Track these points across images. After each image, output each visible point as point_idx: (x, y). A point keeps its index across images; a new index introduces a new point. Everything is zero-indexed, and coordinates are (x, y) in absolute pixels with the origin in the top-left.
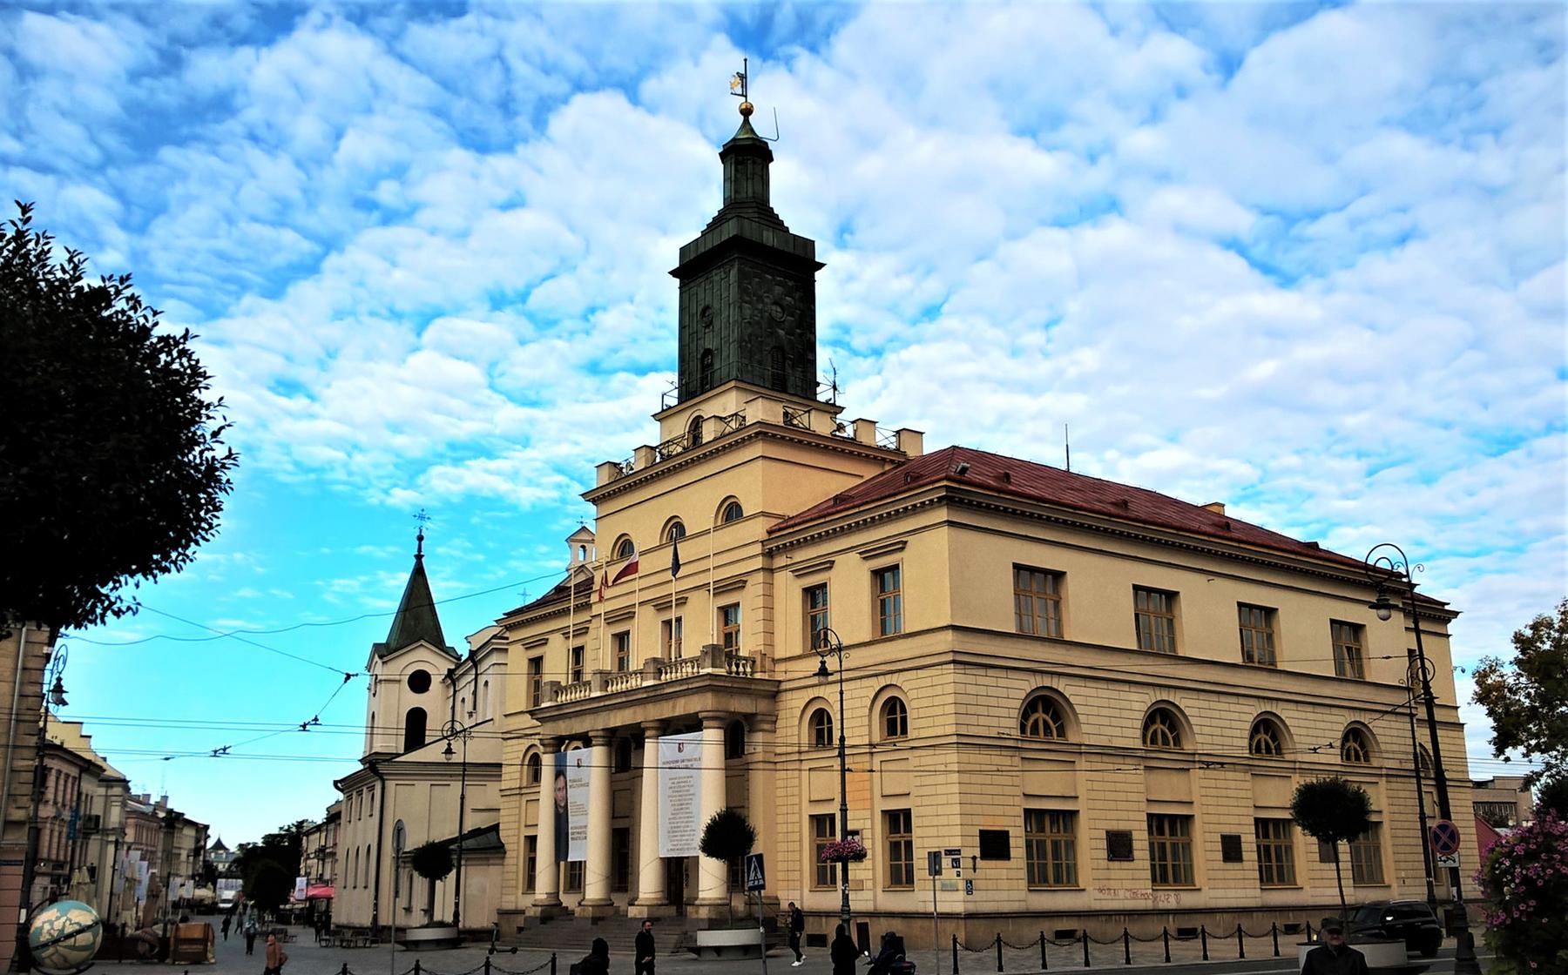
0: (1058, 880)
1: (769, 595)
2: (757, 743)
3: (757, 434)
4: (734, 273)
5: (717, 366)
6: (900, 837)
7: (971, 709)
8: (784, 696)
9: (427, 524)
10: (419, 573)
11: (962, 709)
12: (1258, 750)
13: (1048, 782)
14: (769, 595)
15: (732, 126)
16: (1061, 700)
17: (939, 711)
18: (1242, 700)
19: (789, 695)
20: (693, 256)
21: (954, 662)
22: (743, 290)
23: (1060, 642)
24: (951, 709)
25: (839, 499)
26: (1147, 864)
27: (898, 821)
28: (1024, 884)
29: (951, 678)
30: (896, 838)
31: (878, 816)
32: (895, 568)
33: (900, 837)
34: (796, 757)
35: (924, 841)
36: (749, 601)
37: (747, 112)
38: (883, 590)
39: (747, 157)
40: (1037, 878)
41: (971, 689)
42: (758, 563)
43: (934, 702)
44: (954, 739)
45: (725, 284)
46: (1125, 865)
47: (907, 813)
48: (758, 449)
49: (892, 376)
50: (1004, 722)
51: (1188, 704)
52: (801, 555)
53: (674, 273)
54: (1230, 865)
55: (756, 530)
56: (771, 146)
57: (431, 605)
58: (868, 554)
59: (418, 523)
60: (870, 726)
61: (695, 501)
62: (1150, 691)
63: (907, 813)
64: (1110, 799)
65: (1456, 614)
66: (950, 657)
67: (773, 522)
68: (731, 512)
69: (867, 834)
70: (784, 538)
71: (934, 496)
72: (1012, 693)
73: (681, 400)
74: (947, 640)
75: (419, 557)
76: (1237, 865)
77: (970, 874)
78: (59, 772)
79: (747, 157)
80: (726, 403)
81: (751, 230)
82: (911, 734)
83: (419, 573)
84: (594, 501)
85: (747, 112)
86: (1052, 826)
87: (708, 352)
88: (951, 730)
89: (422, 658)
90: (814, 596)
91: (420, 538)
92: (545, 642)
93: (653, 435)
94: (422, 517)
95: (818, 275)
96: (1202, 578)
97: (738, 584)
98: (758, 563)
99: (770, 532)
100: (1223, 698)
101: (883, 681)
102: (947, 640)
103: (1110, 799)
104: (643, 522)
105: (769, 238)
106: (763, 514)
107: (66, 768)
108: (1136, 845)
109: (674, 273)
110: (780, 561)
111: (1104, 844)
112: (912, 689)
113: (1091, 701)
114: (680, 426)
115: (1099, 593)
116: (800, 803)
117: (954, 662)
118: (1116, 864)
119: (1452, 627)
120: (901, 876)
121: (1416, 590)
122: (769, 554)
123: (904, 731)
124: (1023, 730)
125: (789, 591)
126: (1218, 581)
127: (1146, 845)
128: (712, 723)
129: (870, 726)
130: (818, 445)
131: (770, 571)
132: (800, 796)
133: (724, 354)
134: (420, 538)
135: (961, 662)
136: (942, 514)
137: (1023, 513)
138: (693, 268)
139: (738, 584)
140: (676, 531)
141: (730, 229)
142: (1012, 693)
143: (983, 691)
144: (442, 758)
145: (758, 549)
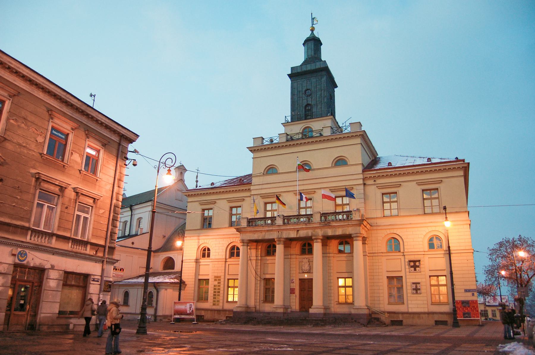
5: (314, 110)
15: (308, 34)
20: (299, 71)
37: (312, 30)
42: (361, 182)
52: (379, 181)
61: (320, 156)
73: (293, 120)
84: (251, 151)
85: (312, 30)
87: (308, 105)
93: (282, 130)
104: (287, 161)
114: (297, 128)
122: (364, 179)
133: (319, 107)
138: (295, 75)
144: (131, 246)
145: (361, 176)
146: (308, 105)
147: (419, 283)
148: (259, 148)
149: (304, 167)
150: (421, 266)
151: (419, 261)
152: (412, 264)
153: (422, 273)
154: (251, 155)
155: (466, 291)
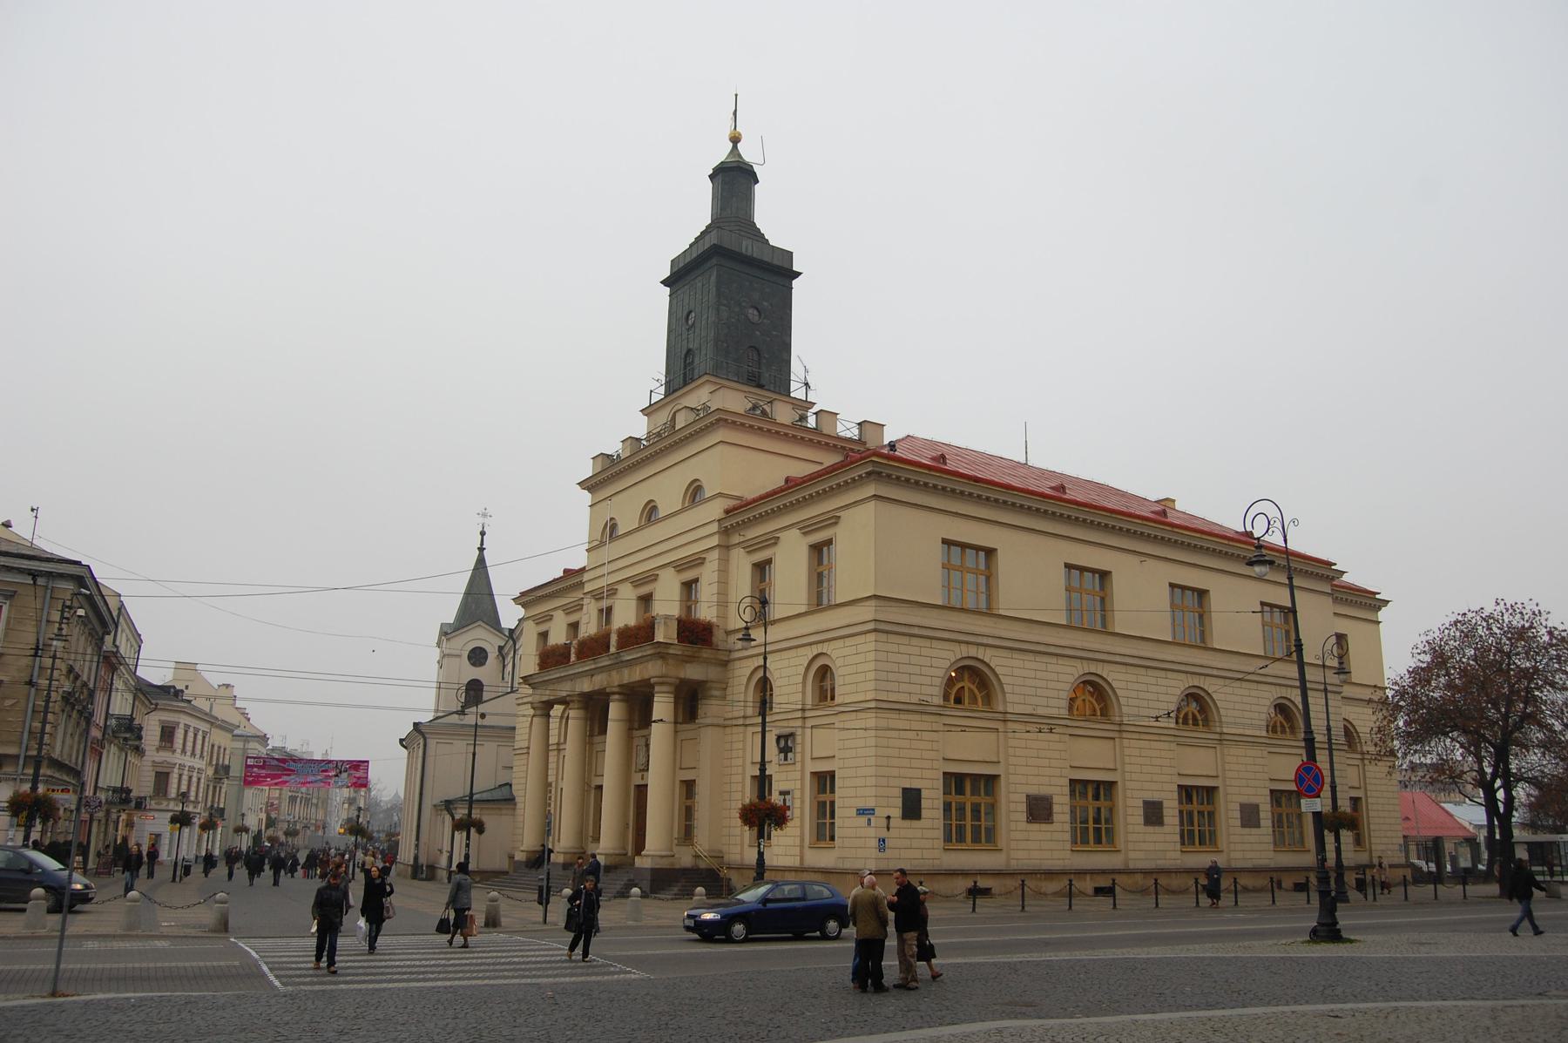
0: (976, 839)
1: (724, 570)
2: (710, 710)
3: (718, 420)
4: (713, 278)
5: (697, 361)
6: (826, 797)
7: (891, 676)
8: (730, 666)
9: (487, 521)
10: (481, 563)
11: (883, 676)
12: (1185, 722)
13: (970, 747)
14: (724, 570)
15: (721, 153)
16: (985, 669)
17: (861, 677)
18: (1170, 674)
19: (737, 664)
21: (875, 630)
22: (719, 294)
23: (989, 613)
24: (871, 675)
25: (791, 484)
26: (1067, 827)
27: (825, 781)
28: (940, 843)
29: (872, 646)
30: (822, 797)
31: (808, 776)
32: (829, 542)
33: (826, 797)
34: (741, 722)
35: (846, 798)
36: (708, 576)
37: (735, 140)
38: (820, 562)
39: (734, 180)
40: (953, 837)
41: (892, 657)
43: (857, 669)
44: (873, 705)
45: (706, 285)
46: (1044, 827)
47: (832, 775)
48: (721, 434)
49: (844, 366)
50: (929, 690)
51: (1116, 677)
52: (752, 533)
53: (665, 283)
54: (1150, 829)
55: (715, 510)
56: (756, 168)
57: (492, 595)
58: (807, 529)
59: (481, 520)
60: (804, 693)
61: (667, 488)
62: (1078, 663)
63: (832, 775)
64: (1035, 764)
65: (799, 274)
66: (871, 626)
67: (731, 503)
68: (694, 493)
69: (797, 794)
70: (741, 515)
71: (862, 472)
72: (935, 662)
74: (866, 612)
75: (481, 549)
76: (1157, 829)
77: (883, 833)
78: (187, 727)
79: (734, 180)
80: (701, 396)
81: (730, 242)
82: (838, 700)
83: (481, 563)
84: (590, 489)
85: (735, 140)
86: (971, 792)
88: (870, 696)
89: (479, 636)
90: (762, 568)
91: (483, 534)
92: (551, 618)
94: (484, 515)
95: (795, 283)
96: (1135, 559)
97: (698, 561)
98: (715, 541)
99: (727, 512)
100: (1150, 672)
101: (815, 650)
102: (866, 612)
103: (1035, 764)
105: (747, 247)
106: (720, 495)
107: (193, 723)
108: (1056, 808)
109: (665, 283)
110: (736, 539)
111: (1024, 807)
112: (842, 657)
113: (1017, 672)
115: (1032, 572)
116: (743, 766)
117: (875, 630)
118: (1035, 827)
119: (1382, 615)
120: (825, 832)
121: (1345, 578)
122: (725, 532)
123: (833, 698)
124: (946, 697)
125: (742, 566)
126: (1150, 563)
127: (1067, 809)
128: (664, 688)
129: (804, 693)
130: (777, 433)
131: (725, 548)
132: (744, 758)
134: (483, 534)
135: (881, 629)
136: (870, 490)
137: (953, 491)
138: (679, 278)
139: (698, 561)
140: (650, 513)
141: (712, 239)
142: (935, 662)
143: (905, 659)
145: (715, 527)
146: (689, 351)
147: (788, 793)
148: (608, 475)
149: (650, 513)
150: (798, 748)
151: (792, 735)
152: (782, 743)
153: (798, 766)
154: (587, 497)
155: (862, 812)
